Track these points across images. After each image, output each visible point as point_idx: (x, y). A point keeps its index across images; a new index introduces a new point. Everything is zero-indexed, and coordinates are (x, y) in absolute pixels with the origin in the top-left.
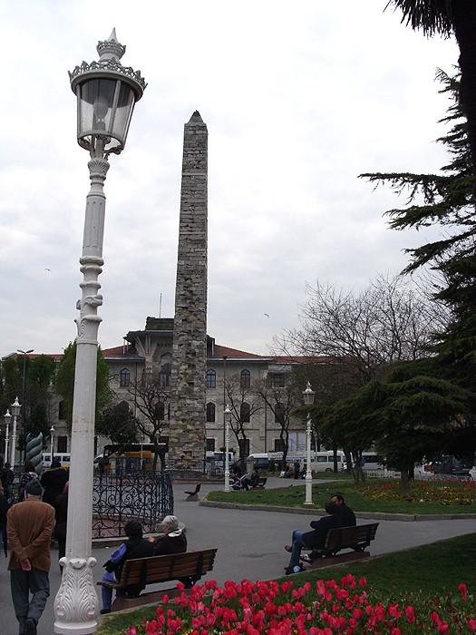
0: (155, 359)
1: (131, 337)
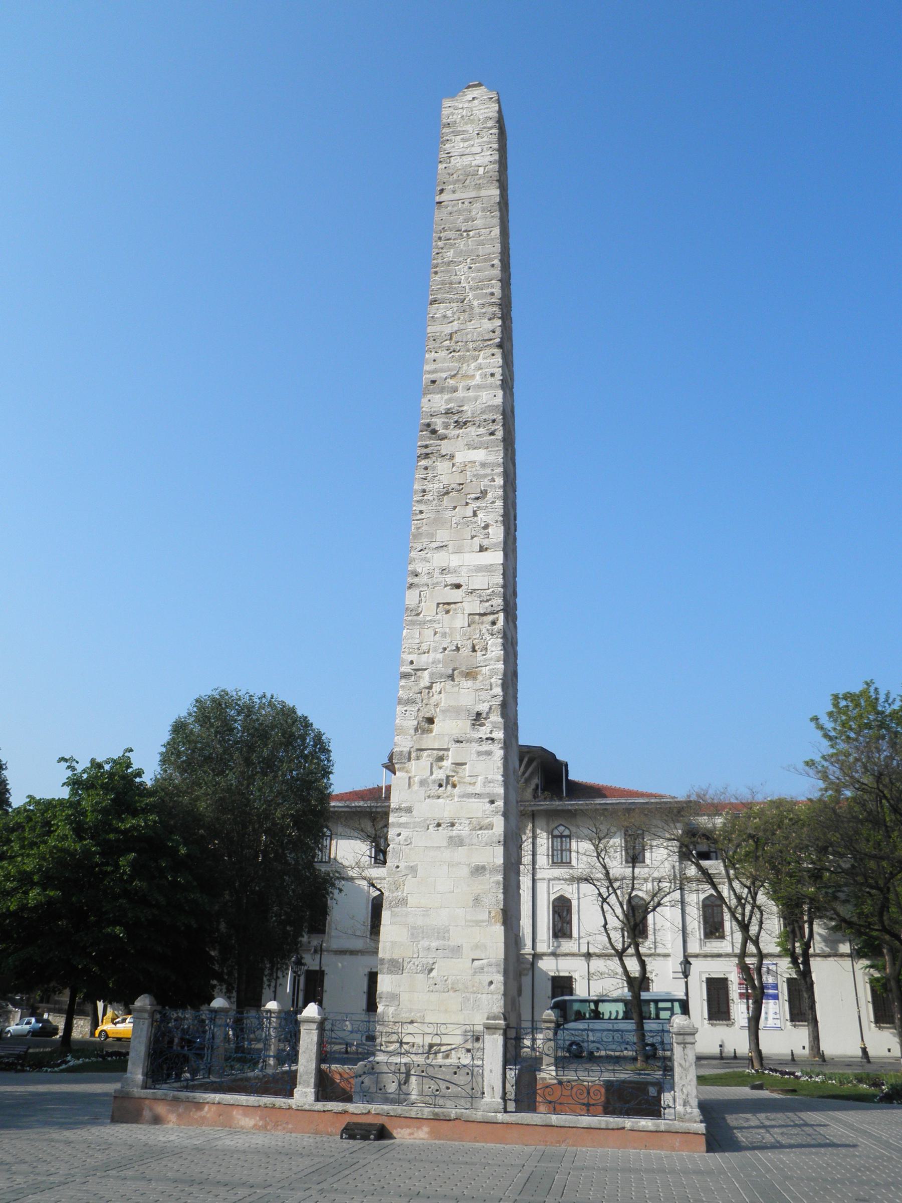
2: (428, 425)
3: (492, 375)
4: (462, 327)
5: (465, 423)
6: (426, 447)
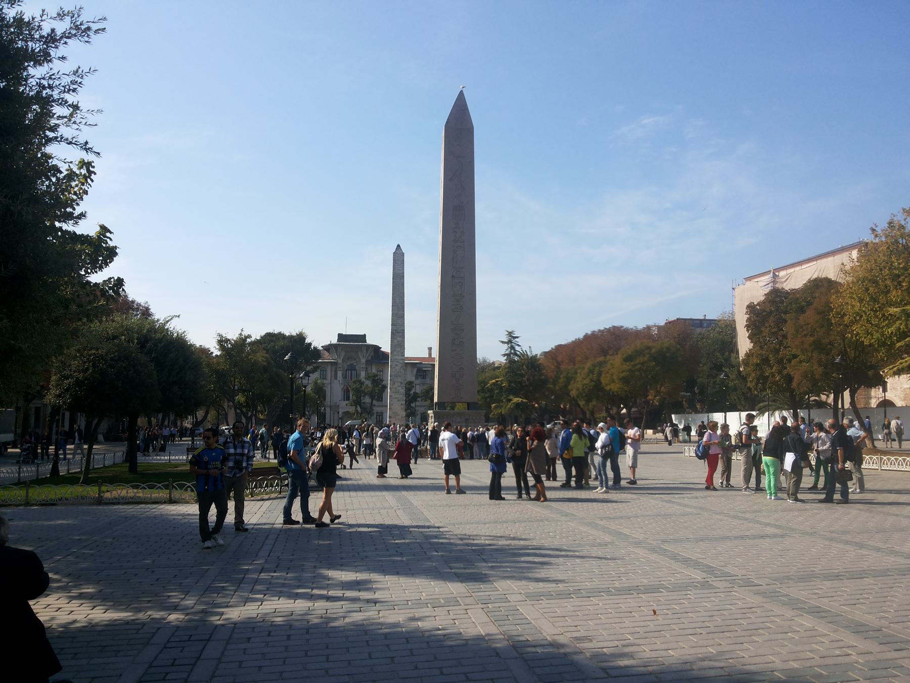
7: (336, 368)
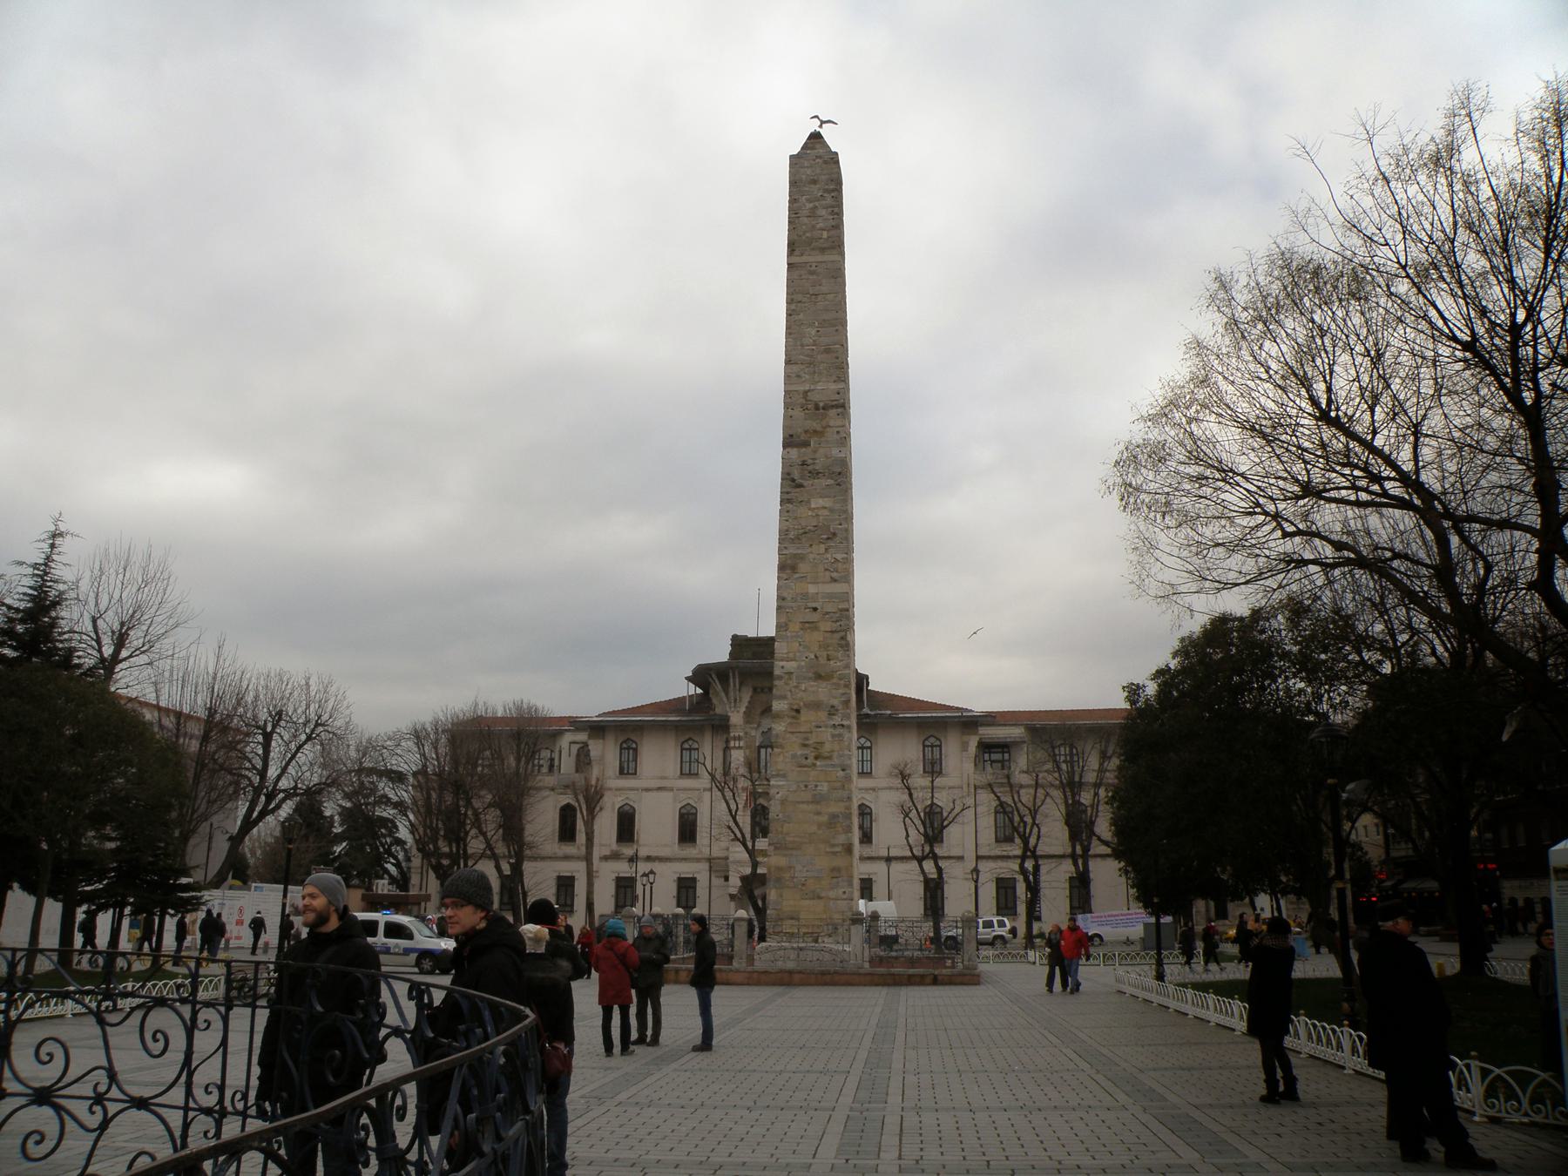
0: (748, 715)
1: (702, 675)
2: (789, 474)
3: (838, 432)
4: (812, 387)
5: (818, 473)
6: (788, 493)
7: (727, 741)
